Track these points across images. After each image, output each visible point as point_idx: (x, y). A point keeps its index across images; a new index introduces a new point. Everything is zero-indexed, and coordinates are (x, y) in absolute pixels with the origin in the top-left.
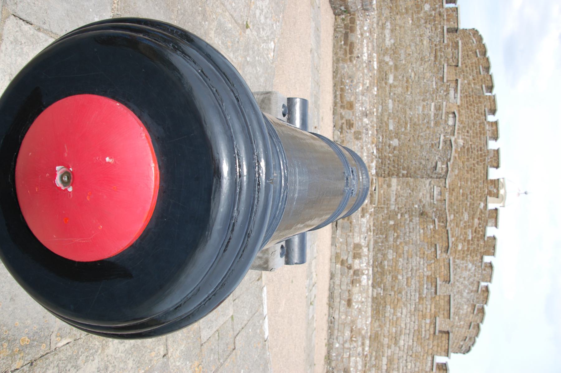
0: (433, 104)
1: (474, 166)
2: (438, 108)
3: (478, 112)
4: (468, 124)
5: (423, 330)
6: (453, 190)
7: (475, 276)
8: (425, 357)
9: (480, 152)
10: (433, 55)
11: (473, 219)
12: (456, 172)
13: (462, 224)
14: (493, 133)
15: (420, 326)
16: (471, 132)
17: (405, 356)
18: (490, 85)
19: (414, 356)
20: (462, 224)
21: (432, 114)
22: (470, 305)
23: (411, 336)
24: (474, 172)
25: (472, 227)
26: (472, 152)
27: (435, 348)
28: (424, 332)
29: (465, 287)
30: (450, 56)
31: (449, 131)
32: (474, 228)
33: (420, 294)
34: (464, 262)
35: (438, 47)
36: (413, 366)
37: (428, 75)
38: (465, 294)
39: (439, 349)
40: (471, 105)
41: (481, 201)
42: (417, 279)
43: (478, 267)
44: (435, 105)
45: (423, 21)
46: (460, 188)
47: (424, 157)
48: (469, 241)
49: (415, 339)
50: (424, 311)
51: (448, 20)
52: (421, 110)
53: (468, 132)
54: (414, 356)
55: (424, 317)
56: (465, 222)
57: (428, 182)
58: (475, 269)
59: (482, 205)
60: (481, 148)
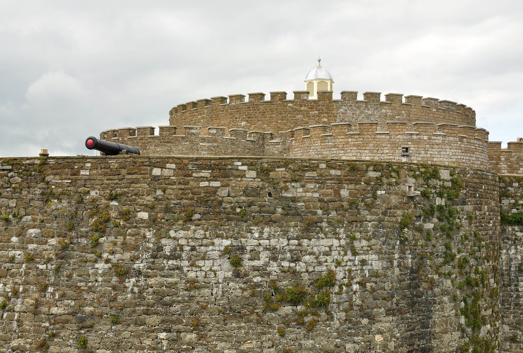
0: (200, 144)
1: (261, 112)
2: (203, 140)
3: (223, 111)
4: (231, 118)
5: (356, 143)
6: (279, 128)
7: (350, 106)
8: (378, 140)
9: (251, 109)
10: (167, 144)
11: (301, 111)
12: (265, 126)
13: (306, 119)
14: (238, 99)
15: (354, 145)
16: (236, 116)
17: (379, 155)
18: (204, 101)
19: (378, 148)
20: (306, 119)
21: (208, 144)
22: (382, 107)
23: (360, 151)
24: (265, 112)
25: (308, 111)
26: (251, 114)
27: (370, 133)
28: (358, 142)
29: (362, 112)
30: (168, 133)
31: (221, 132)
32: (309, 110)
33: (332, 148)
34: (338, 115)
35: (162, 141)
36: (385, 148)
37: (180, 148)
38: (370, 112)
39: (370, 130)
40: (218, 116)
41: (287, 106)
42: (323, 150)
43: (343, 104)
44: (201, 142)
45: (145, 151)
46: (277, 122)
47: (243, 150)
48: (319, 113)
49: (364, 148)
50: (343, 143)
51: (145, 134)
52: (205, 152)
53: (236, 118)
54: (378, 148)
55: (347, 143)
56: (304, 117)
57: (267, 147)
58: (344, 106)
59: (290, 105)
60: (248, 108)
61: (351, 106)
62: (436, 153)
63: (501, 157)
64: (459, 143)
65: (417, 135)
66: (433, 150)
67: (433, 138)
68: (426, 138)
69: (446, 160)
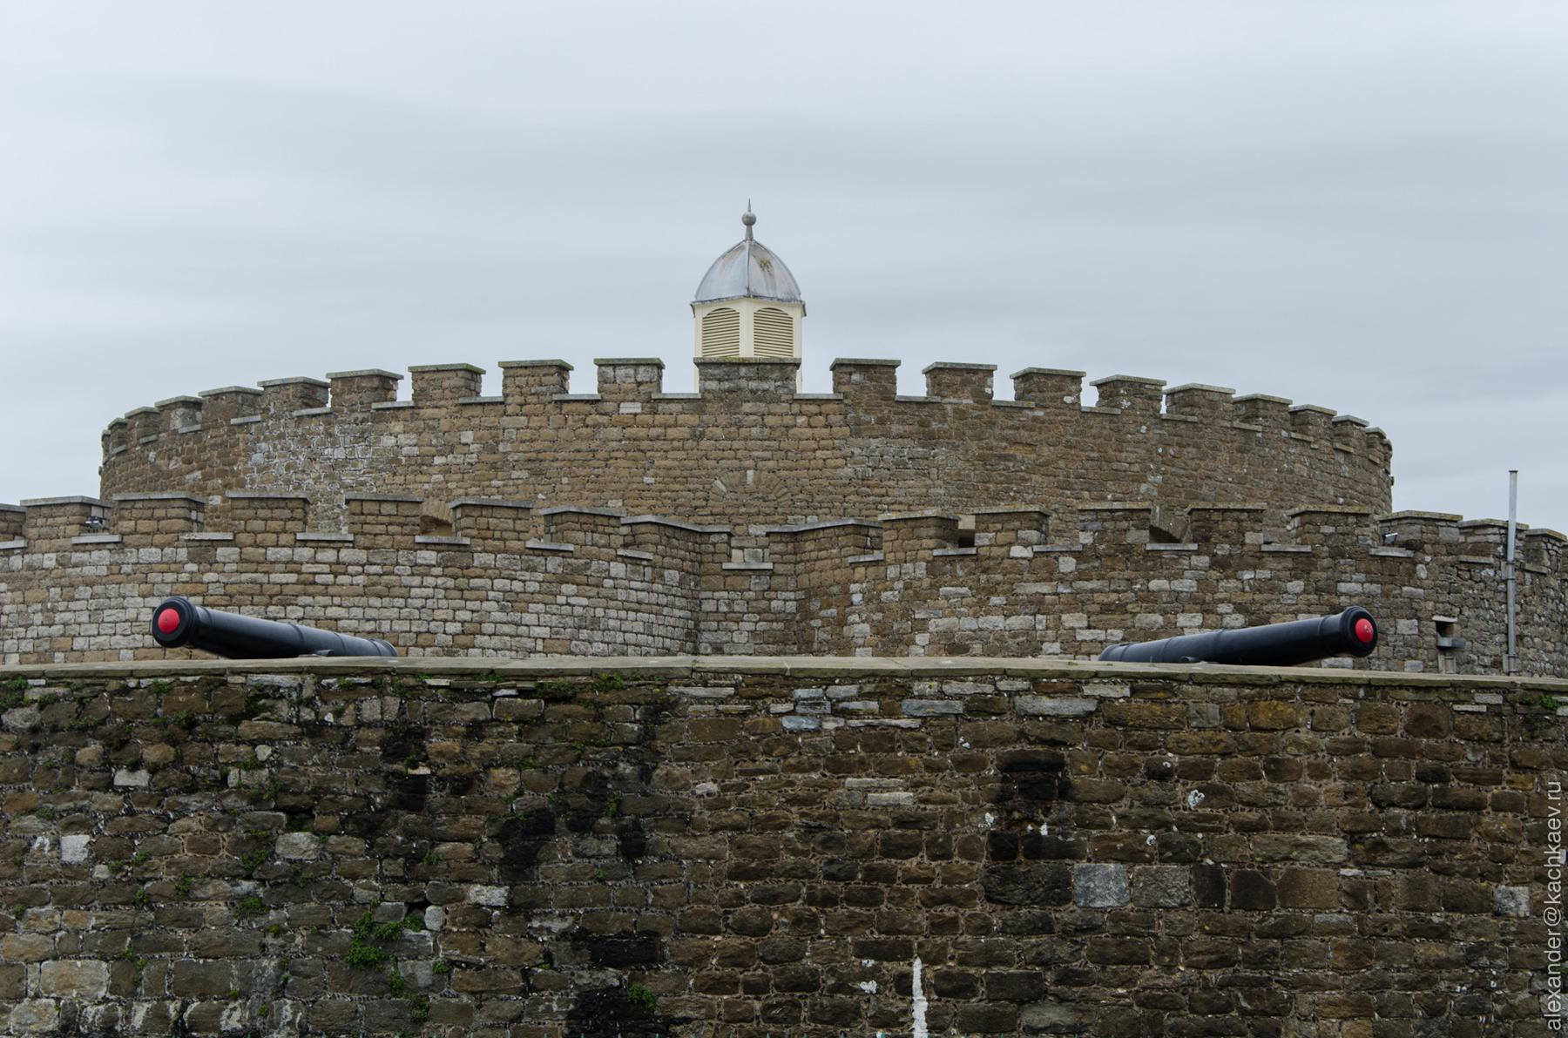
7: (281, 436)
22: (383, 426)
38: (339, 454)
58: (266, 440)
61: (281, 436)
62: (84, 618)
63: (854, 587)
64: (192, 567)
65: (24, 551)
66: (72, 605)
67: (77, 557)
68: (49, 561)
69: (124, 642)
